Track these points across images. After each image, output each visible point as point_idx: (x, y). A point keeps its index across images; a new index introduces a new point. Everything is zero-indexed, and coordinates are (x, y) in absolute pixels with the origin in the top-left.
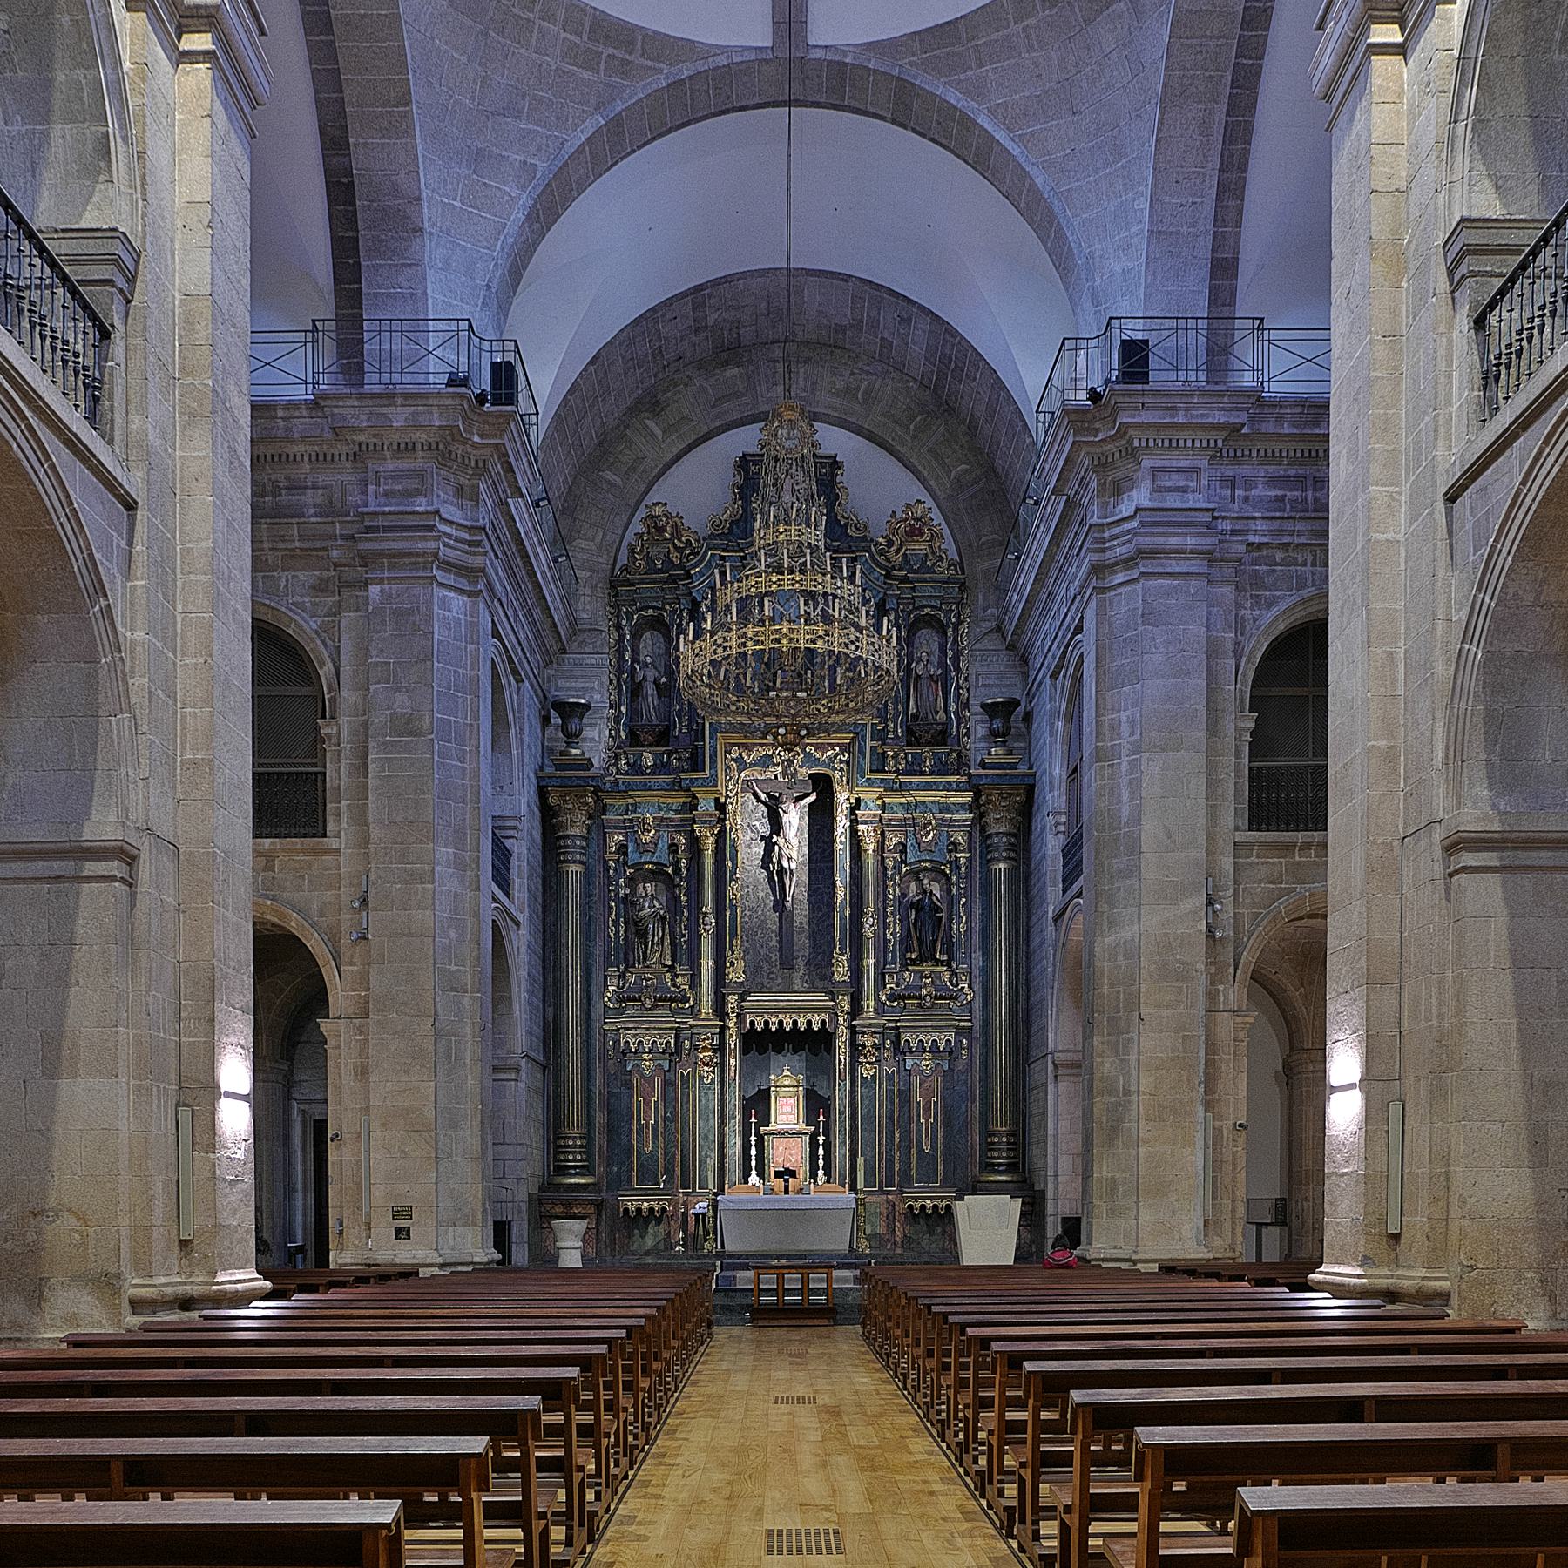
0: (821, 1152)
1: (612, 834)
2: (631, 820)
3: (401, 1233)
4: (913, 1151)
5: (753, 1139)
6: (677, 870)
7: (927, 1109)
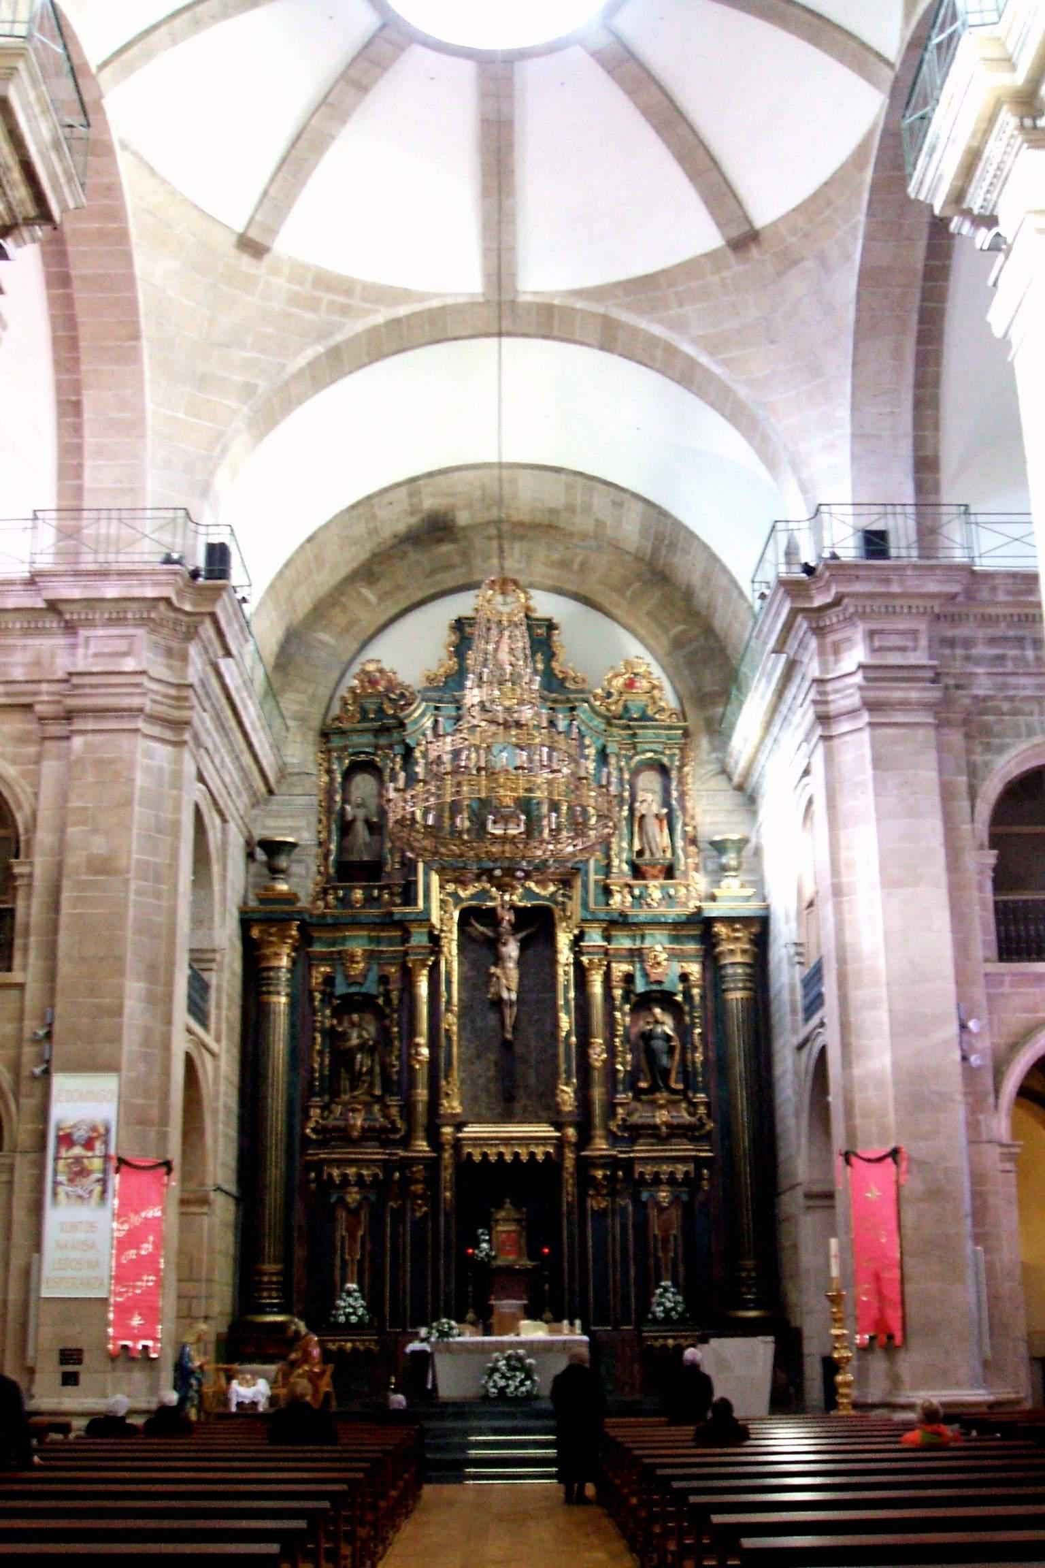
1: (318, 966)
2: (340, 952)
3: (70, 1379)
6: (388, 1001)
7: (665, 1240)
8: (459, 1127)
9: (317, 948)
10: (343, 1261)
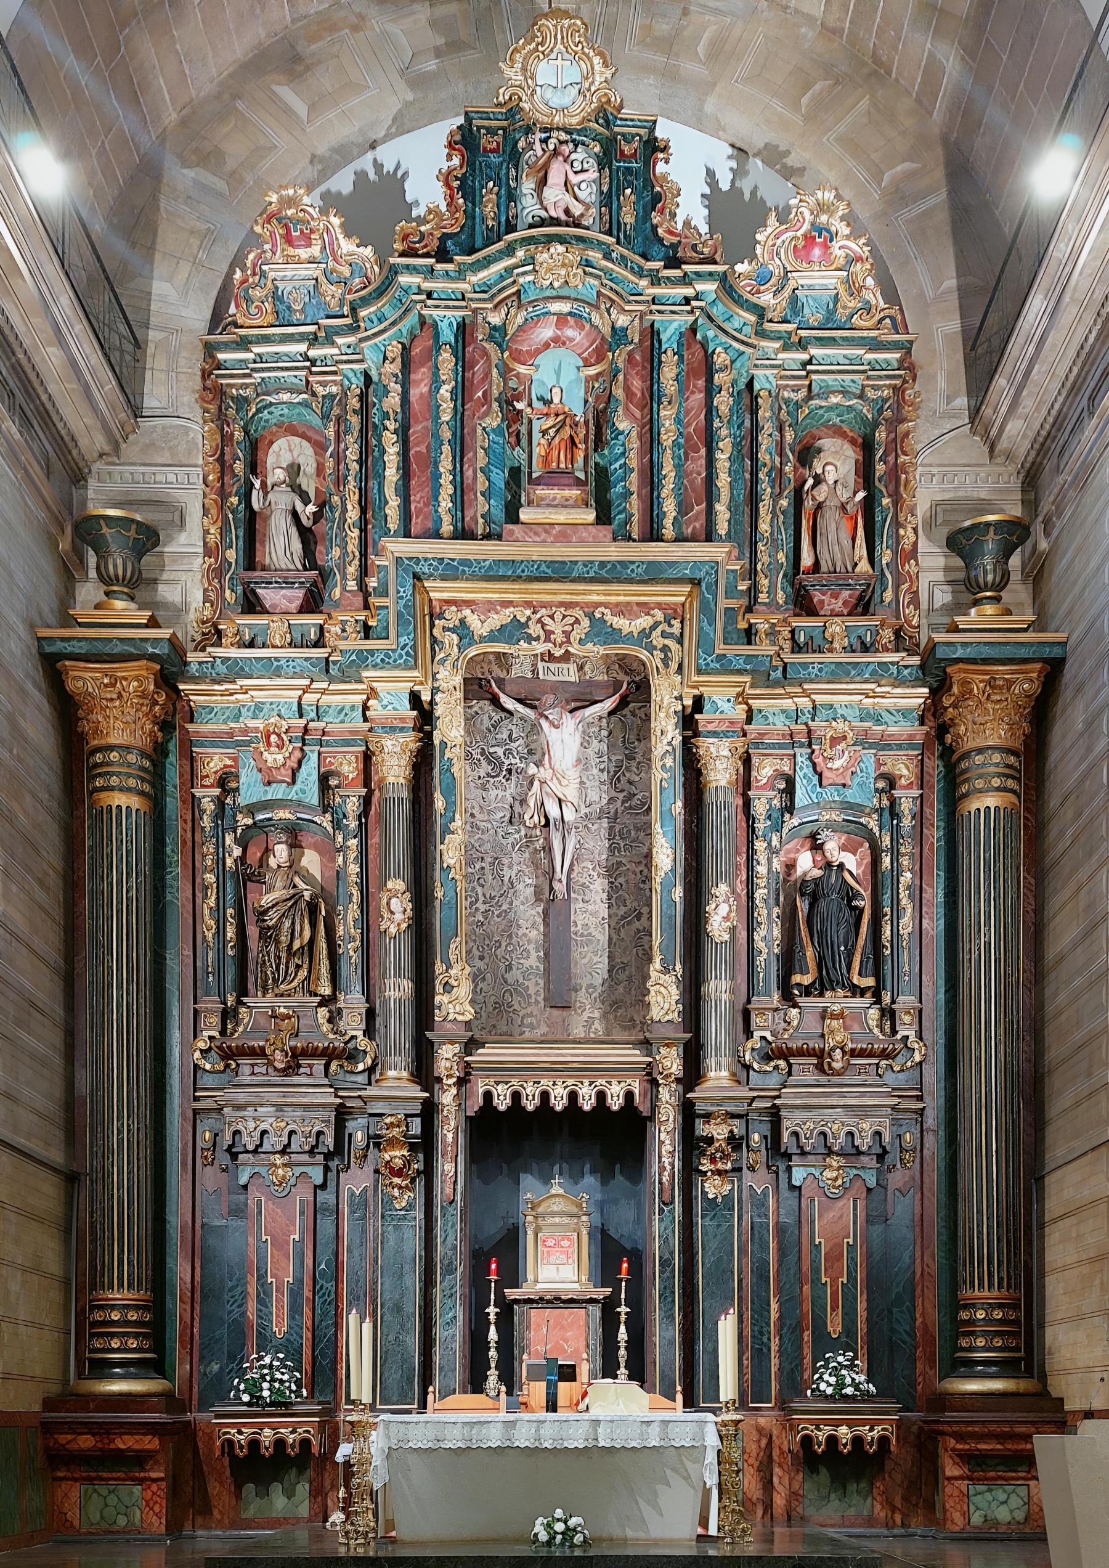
0: (623, 1334)
4: (807, 1336)
5: (492, 1310)
8: (471, 1045)
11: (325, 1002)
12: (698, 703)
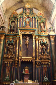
8: (21, 57)
9: (7, 38)
10: (7, 73)
11: (12, 54)
12: (36, 37)
